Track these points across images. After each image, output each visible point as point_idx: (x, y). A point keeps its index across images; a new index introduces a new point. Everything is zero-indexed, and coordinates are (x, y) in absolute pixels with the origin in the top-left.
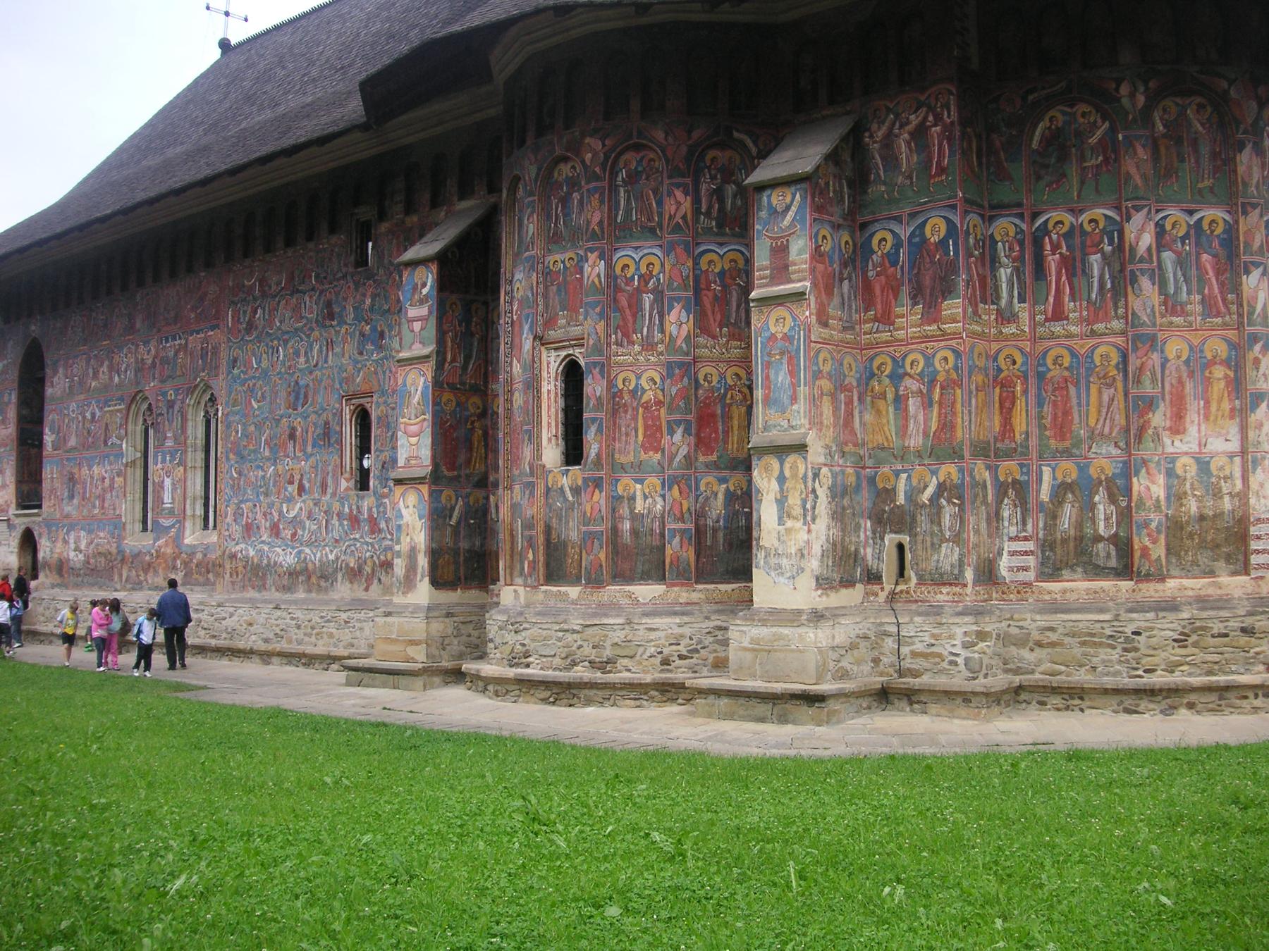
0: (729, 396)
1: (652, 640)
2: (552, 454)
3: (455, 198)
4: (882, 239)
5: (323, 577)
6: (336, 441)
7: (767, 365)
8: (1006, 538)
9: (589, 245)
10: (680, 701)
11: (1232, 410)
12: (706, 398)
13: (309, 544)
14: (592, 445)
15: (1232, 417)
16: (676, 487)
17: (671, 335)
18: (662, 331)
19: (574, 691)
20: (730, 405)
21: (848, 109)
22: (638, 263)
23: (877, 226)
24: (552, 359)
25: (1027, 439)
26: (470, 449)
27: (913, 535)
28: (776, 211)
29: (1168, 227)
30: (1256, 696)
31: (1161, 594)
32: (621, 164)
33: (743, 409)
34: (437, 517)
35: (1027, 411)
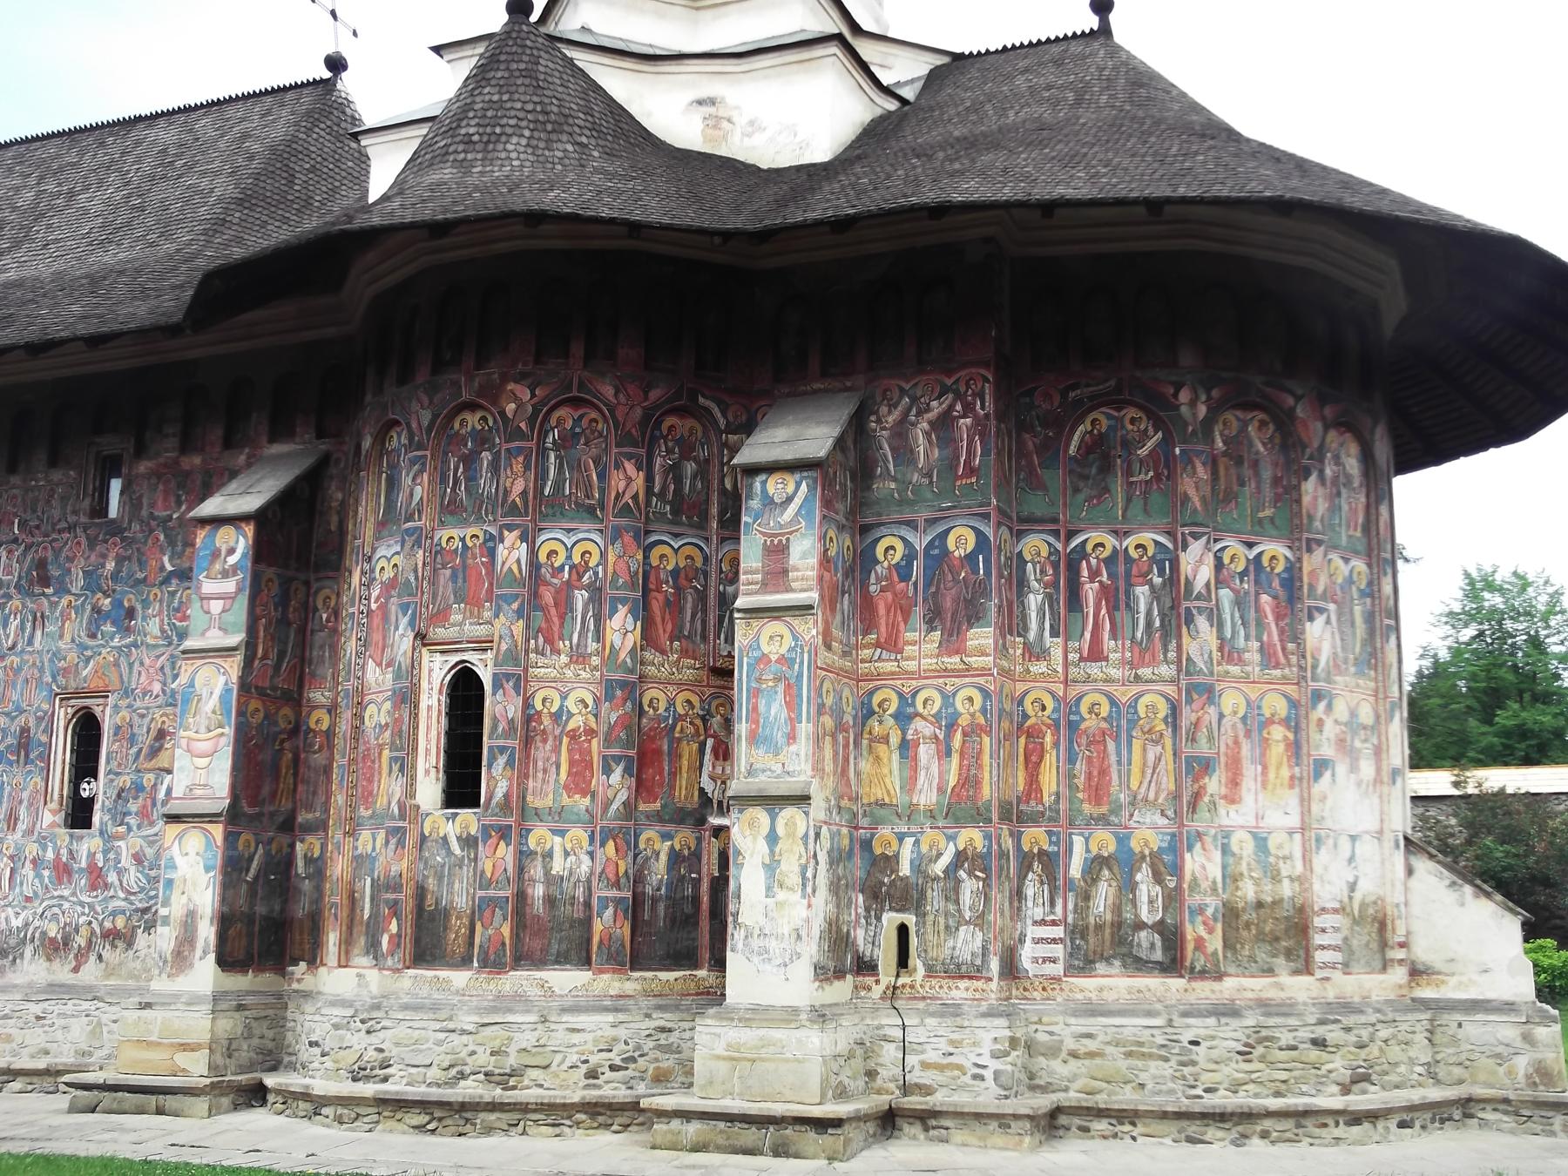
0: (678, 728)
1: (574, 1045)
2: (430, 790)
3: (264, 439)
4: (890, 547)
6: (40, 757)
7: (755, 693)
8: (1029, 922)
9: (508, 520)
10: (615, 1127)
11: (1292, 778)
12: (650, 729)
14: (495, 780)
15: (1291, 787)
16: (611, 844)
17: (612, 646)
18: (599, 636)
19: (468, 1115)
20: (679, 740)
21: (848, 384)
22: (569, 550)
23: (884, 530)
24: (436, 666)
25: (1057, 801)
26: (276, 777)
27: (921, 915)
28: (772, 501)
29: (1226, 561)
30: (1337, 1124)
31: (1219, 996)
32: (553, 422)
33: (695, 746)
34: (232, 867)
35: (1058, 767)
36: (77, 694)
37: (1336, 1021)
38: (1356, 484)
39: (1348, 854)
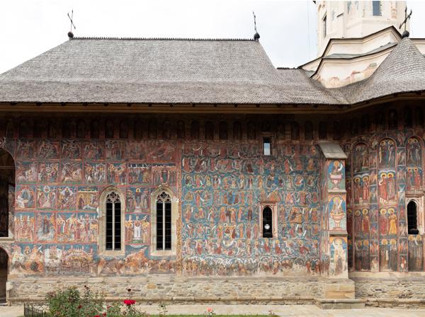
5: (251, 270)
13: (239, 257)
36: (266, 202)
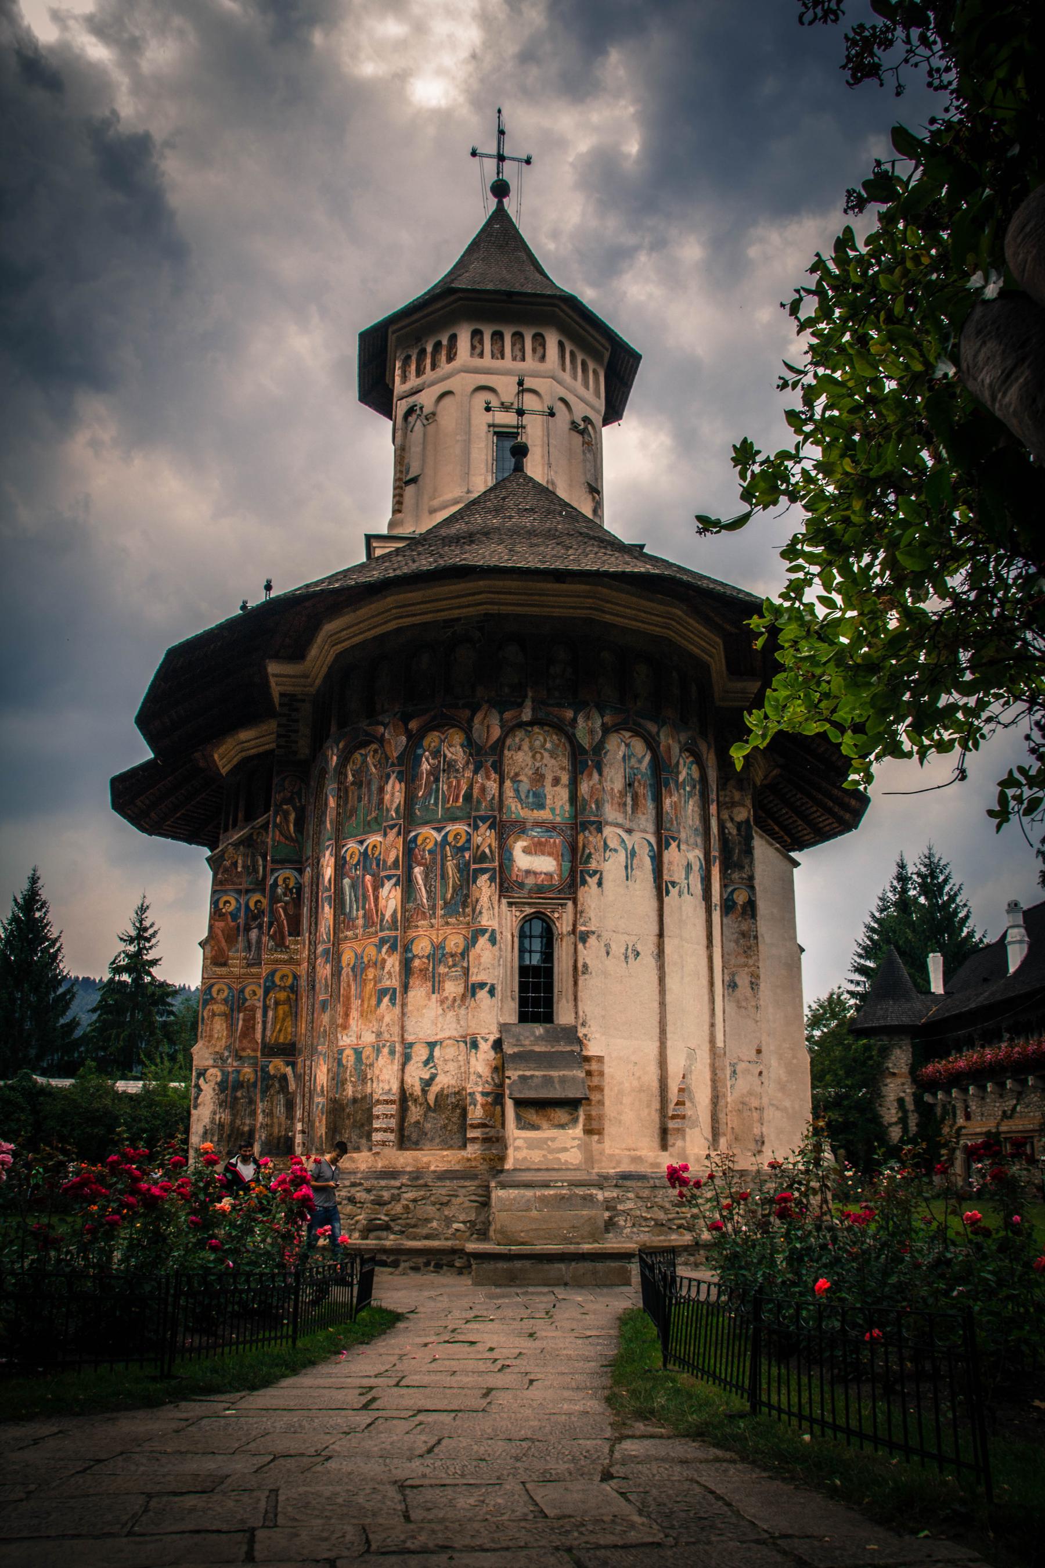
29: (348, 859)
37: (361, 1184)
38: (460, 765)
39: (424, 1058)
